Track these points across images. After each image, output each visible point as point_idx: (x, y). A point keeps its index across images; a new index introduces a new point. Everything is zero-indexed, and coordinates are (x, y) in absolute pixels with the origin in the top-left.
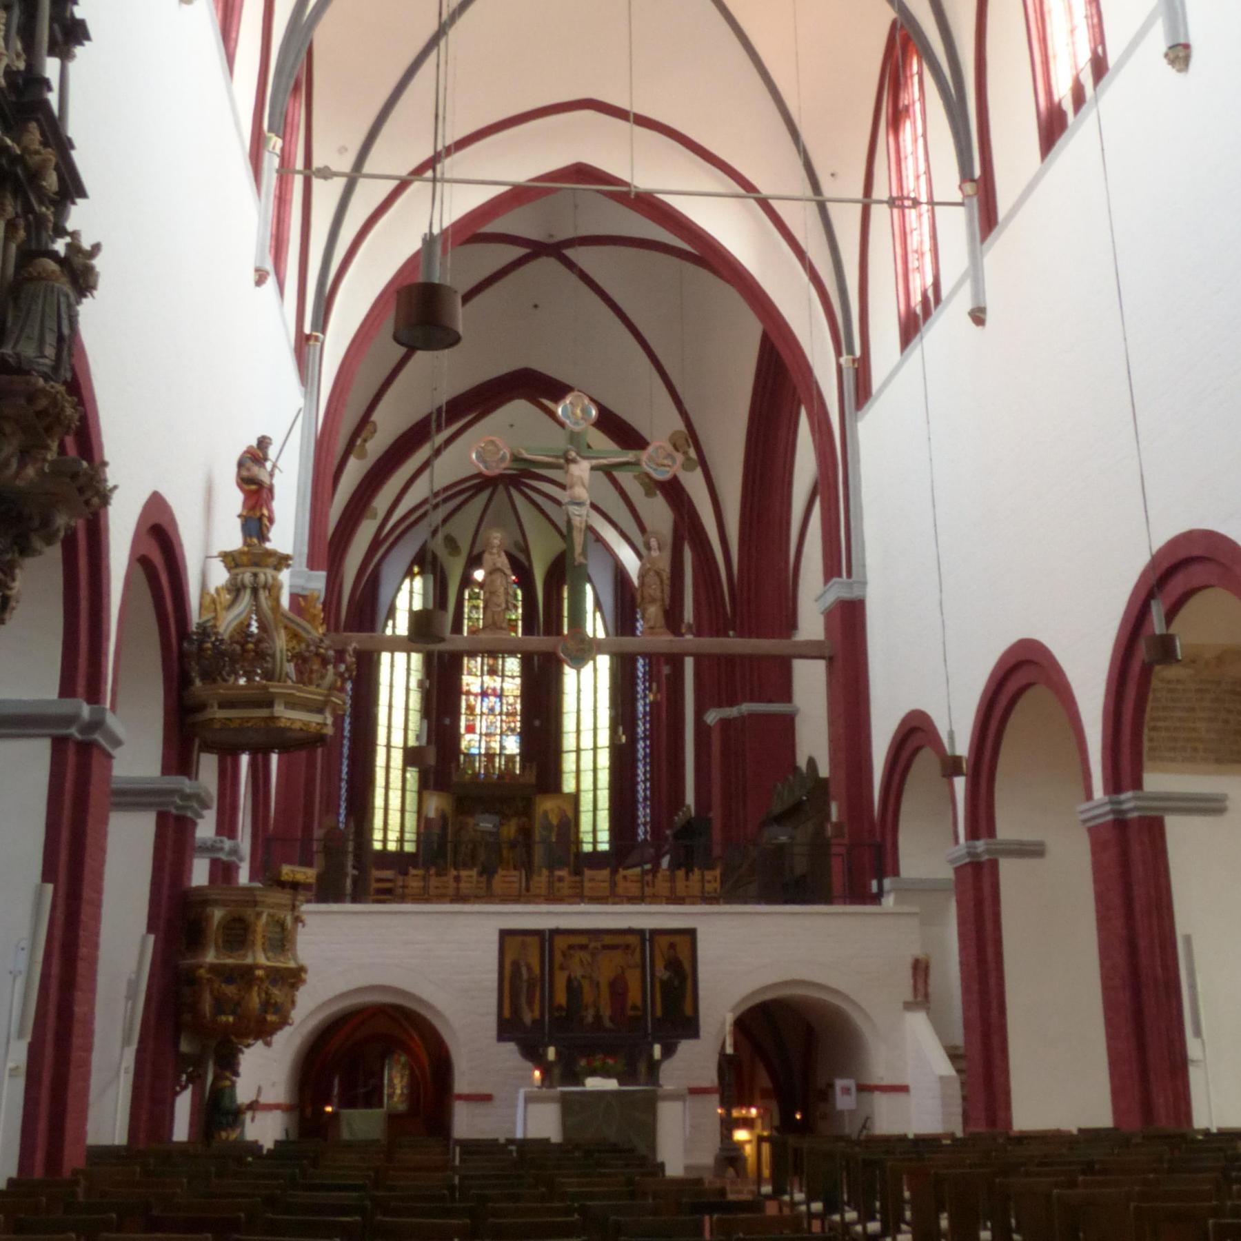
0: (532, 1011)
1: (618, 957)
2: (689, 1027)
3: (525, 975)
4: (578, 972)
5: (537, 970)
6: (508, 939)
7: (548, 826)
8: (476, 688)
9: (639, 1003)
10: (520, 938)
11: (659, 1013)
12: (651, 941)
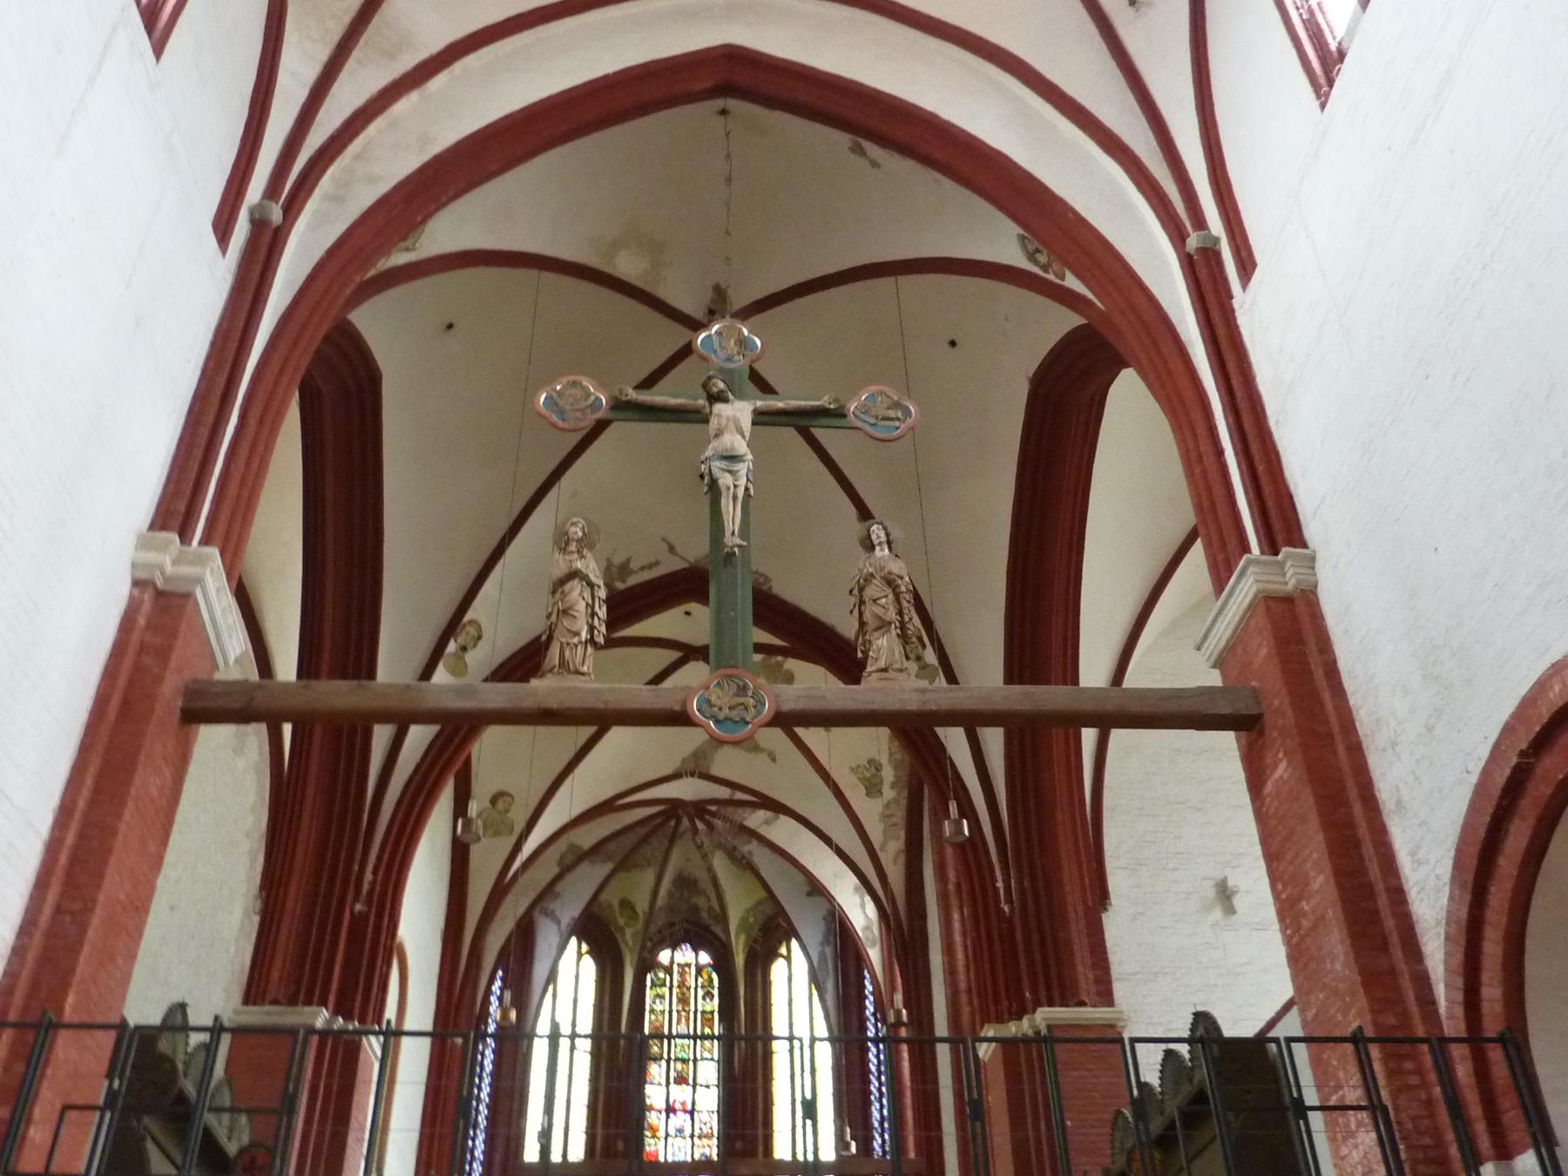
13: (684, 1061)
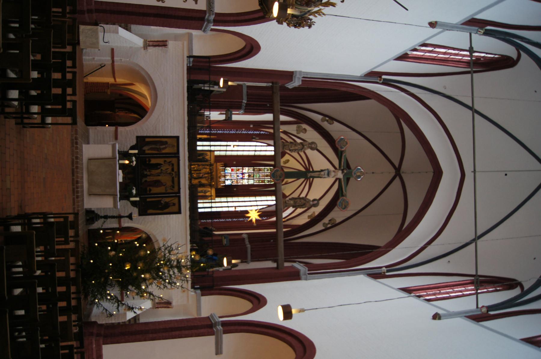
0: (148, 150)
1: (169, 183)
2: (143, 213)
3: (162, 147)
4: (163, 168)
5: (164, 151)
6: (175, 139)
7: (205, 192)
8: (244, 171)
9: (152, 192)
10: (176, 144)
11: (148, 200)
12: (176, 196)
13: (253, 177)
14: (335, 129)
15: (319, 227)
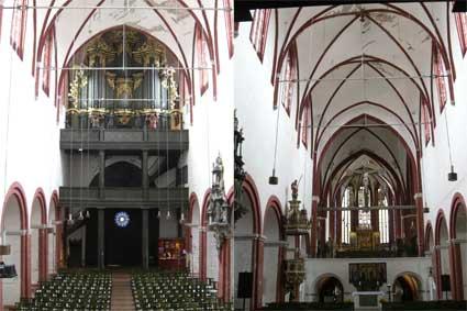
2: (385, 281)
14: (337, 162)
15: (397, 171)
